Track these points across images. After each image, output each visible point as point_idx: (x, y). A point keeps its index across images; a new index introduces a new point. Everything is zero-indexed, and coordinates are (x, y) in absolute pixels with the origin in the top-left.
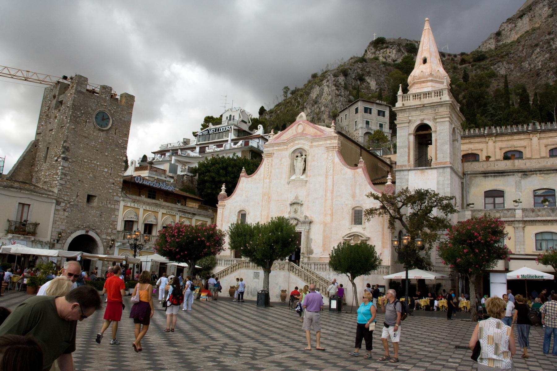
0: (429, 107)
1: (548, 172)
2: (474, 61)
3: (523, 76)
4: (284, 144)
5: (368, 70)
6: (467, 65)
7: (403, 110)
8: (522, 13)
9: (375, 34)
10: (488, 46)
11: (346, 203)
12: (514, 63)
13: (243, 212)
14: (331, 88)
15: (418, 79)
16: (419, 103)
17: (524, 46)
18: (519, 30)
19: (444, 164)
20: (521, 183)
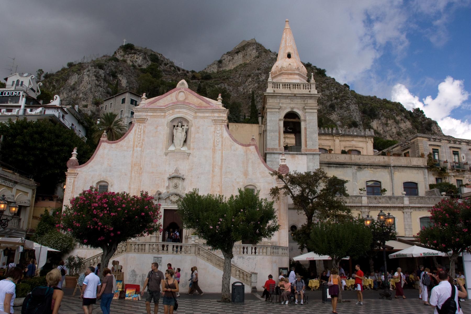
0: (299, 98)
1: (376, 167)
2: (202, 79)
3: (238, 97)
4: (161, 110)
5: (120, 69)
6: (197, 81)
7: (274, 96)
8: (238, 50)
9: (125, 40)
10: (212, 70)
11: (237, 180)
12: (233, 86)
13: (103, 184)
14: (91, 78)
15: (286, 71)
16: (290, 92)
17: (240, 74)
18: (235, 62)
19: (313, 151)
20: (356, 174)
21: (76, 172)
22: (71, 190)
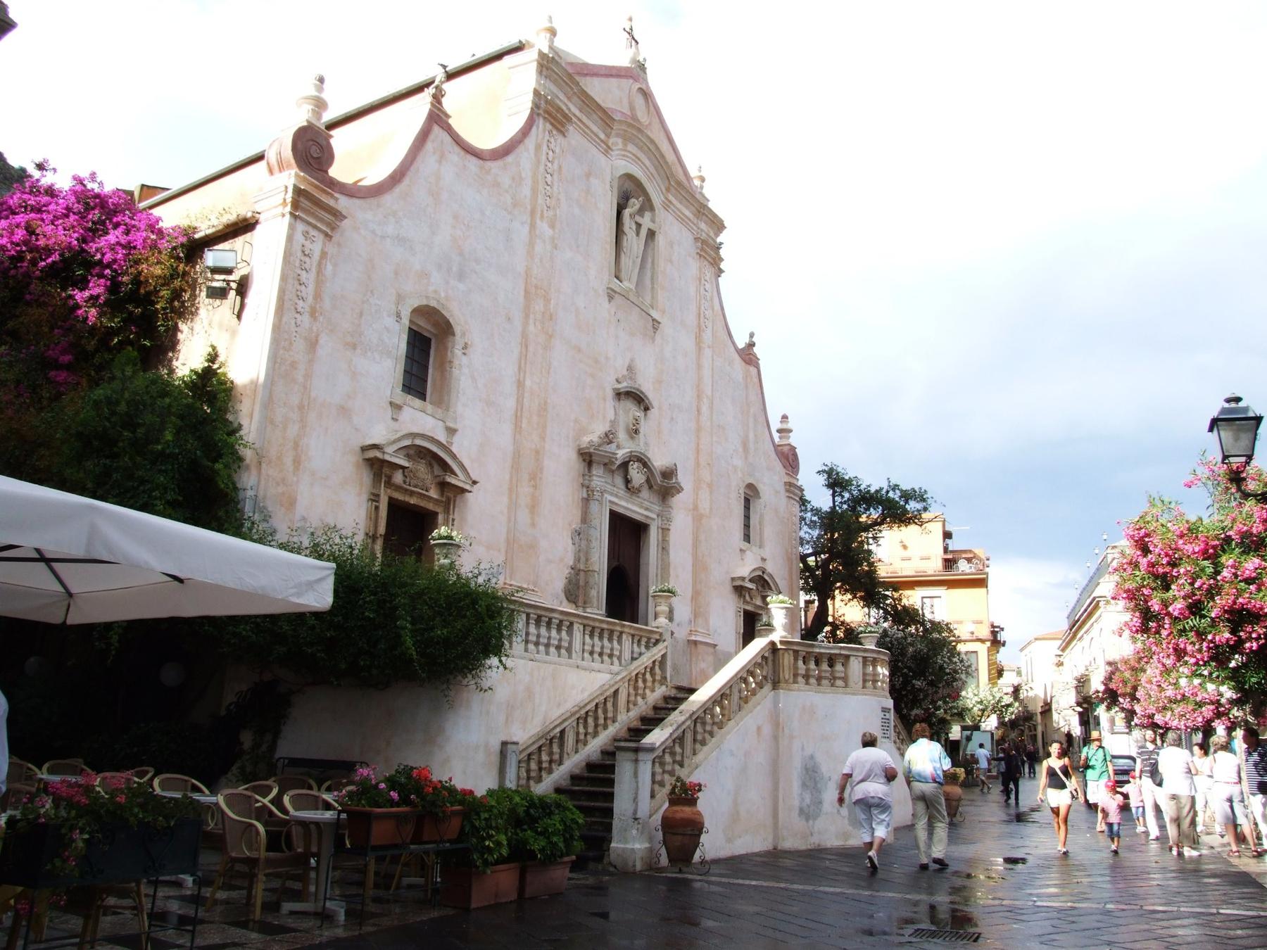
21: (331, 203)
22: (310, 299)
